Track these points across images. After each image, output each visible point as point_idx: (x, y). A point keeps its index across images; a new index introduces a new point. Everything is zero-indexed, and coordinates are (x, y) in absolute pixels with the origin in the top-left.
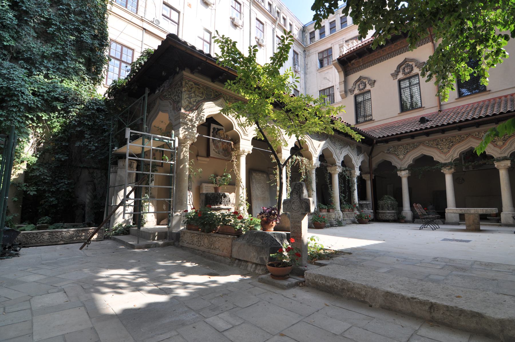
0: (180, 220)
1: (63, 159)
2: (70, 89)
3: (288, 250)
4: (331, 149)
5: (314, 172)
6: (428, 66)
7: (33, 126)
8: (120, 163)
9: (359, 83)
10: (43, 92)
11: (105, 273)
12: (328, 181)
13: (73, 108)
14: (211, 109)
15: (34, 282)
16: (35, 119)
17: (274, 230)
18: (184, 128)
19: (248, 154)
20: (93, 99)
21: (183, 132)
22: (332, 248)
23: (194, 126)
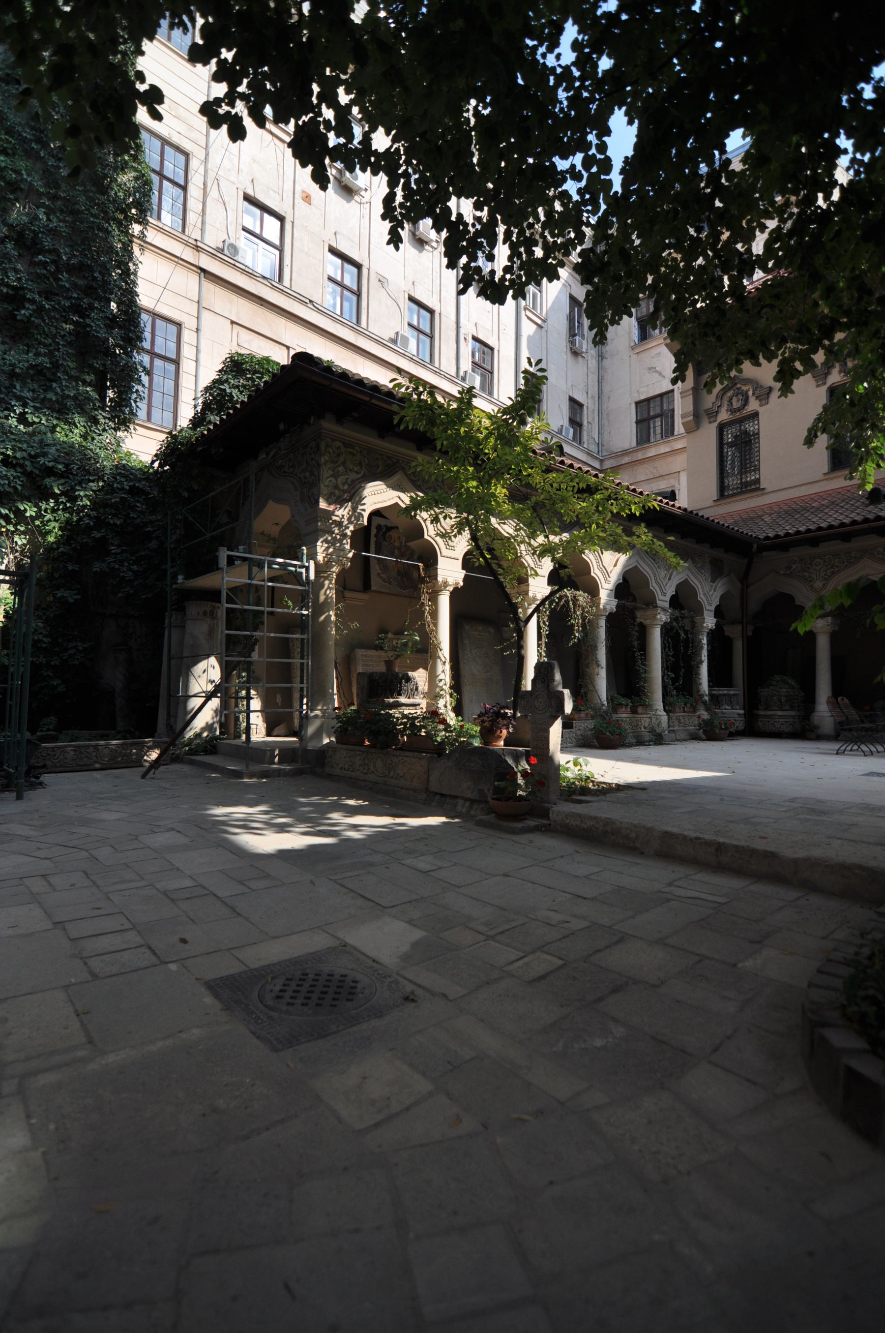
1: (71, 600)
2: (72, 445)
3: (525, 774)
5: (602, 622)
6: (820, 425)
7: (8, 530)
8: (193, 609)
9: (730, 393)
10: (24, 458)
12: (636, 644)
13: (85, 489)
16: (12, 516)
17: (505, 745)
18: (326, 541)
21: (323, 548)
22: (608, 779)
23: (344, 536)
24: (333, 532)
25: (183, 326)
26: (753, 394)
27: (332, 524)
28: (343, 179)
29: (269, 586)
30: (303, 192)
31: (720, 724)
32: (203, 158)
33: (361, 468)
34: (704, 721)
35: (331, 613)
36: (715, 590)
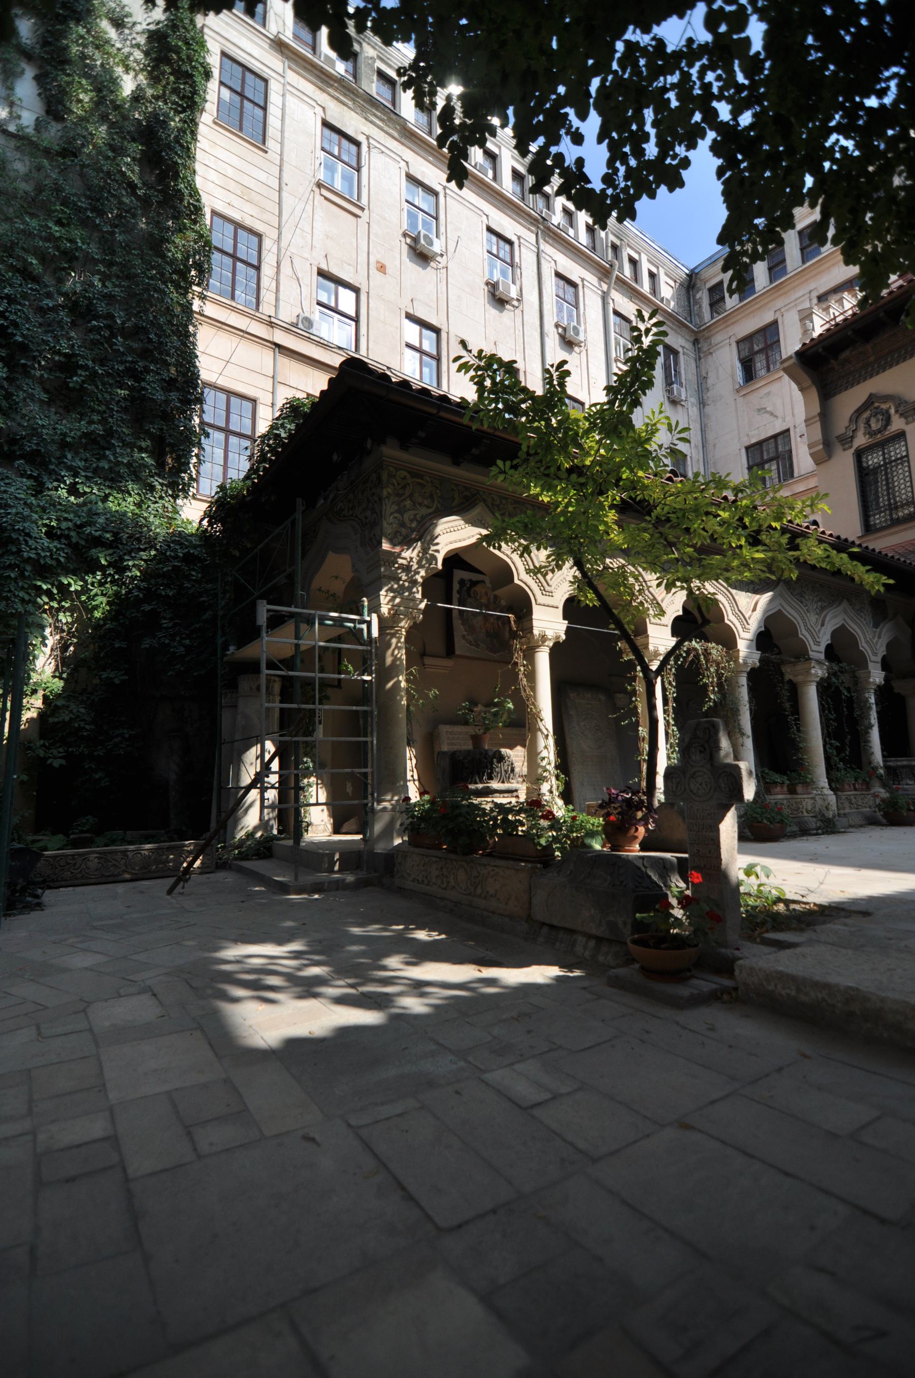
0: (391, 823)
1: (117, 681)
3: (684, 902)
4: (792, 613)
5: (743, 680)
8: (245, 684)
9: (866, 414)
10: (69, 529)
11: (234, 952)
12: (787, 705)
13: (133, 558)
14: (454, 534)
15: (86, 968)
16: (55, 591)
17: (643, 849)
18: (391, 590)
19: (557, 644)
20: (173, 534)
21: (388, 598)
23: (414, 583)
24: (400, 579)
25: (258, 402)
26: (896, 412)
27: (398, 568)
28: (418, 247)
29: (320, 647)
30: (378, 262)
31: (908, 804)
32: (276, 238)
33: (433, 501)
34: (883, 800)
35: (401, 678)
36: (879, 637)
